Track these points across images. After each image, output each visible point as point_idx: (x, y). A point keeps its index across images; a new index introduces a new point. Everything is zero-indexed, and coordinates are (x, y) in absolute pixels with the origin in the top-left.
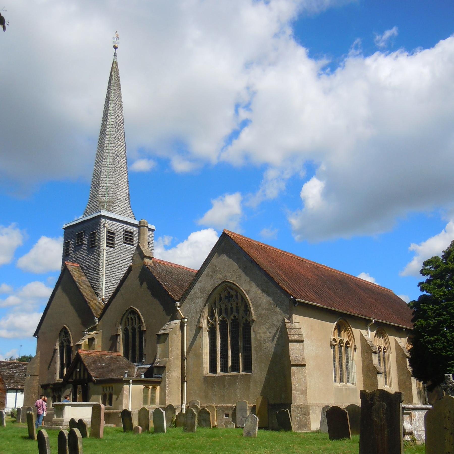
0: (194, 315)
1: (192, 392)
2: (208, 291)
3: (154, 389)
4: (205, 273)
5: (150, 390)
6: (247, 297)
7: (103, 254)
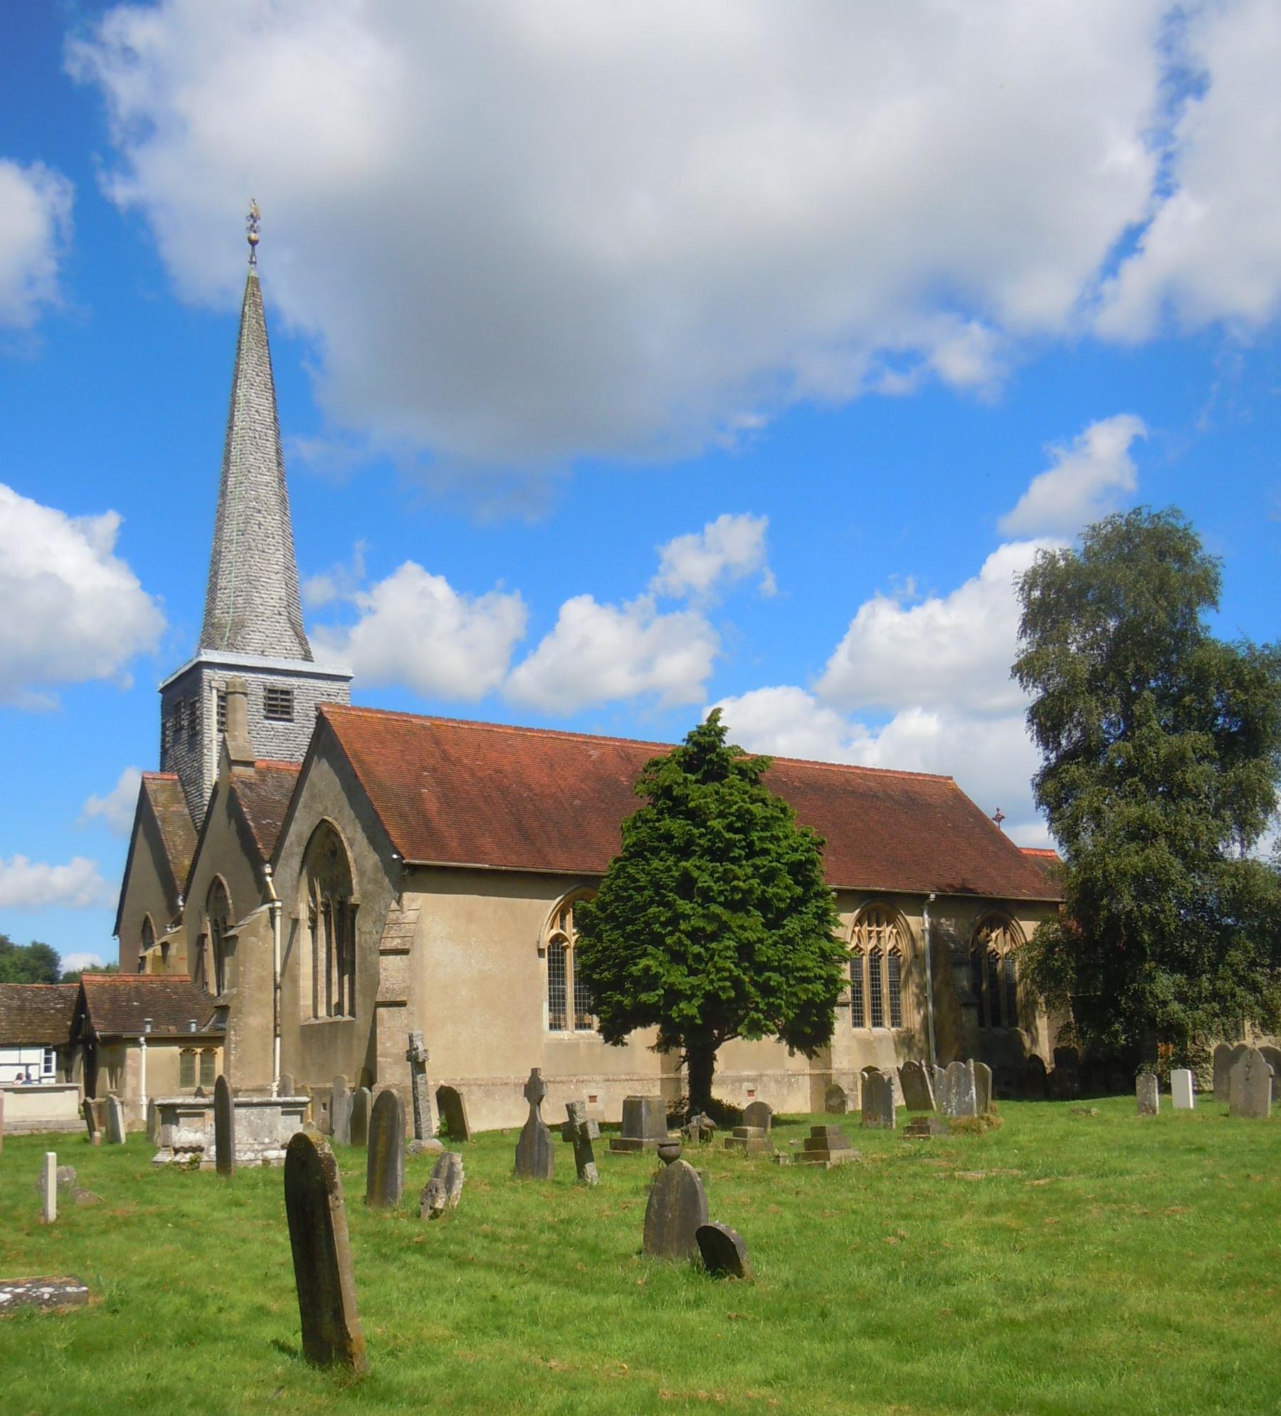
3: (209, 1055)
5: (198, 1057)
6: (349, 854)
7: (210, 750)
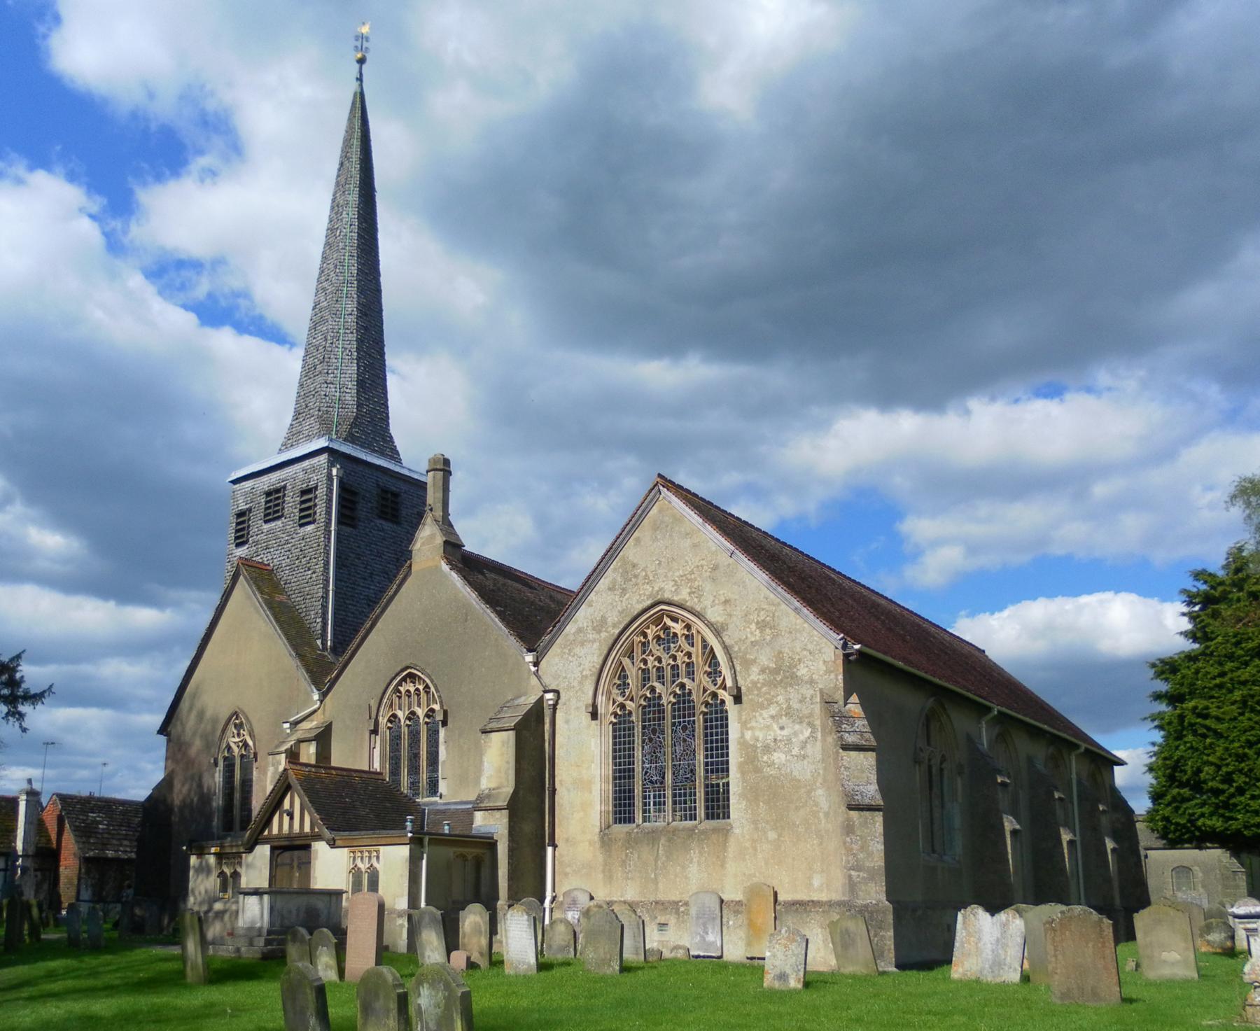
0: (575, 684)
1: (568, 870)
2: (614, 626)
4: (603, 583)
